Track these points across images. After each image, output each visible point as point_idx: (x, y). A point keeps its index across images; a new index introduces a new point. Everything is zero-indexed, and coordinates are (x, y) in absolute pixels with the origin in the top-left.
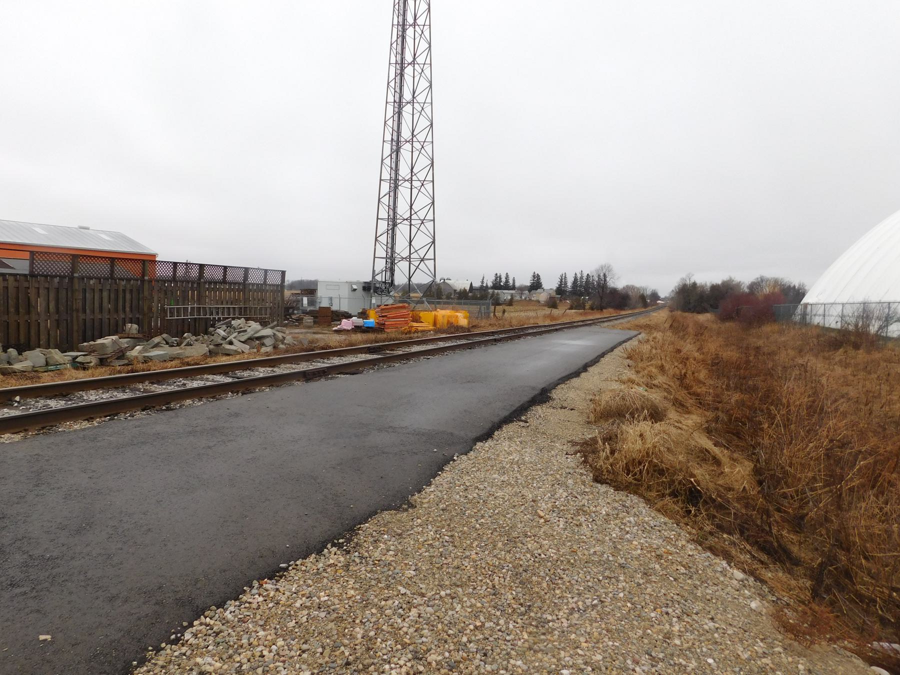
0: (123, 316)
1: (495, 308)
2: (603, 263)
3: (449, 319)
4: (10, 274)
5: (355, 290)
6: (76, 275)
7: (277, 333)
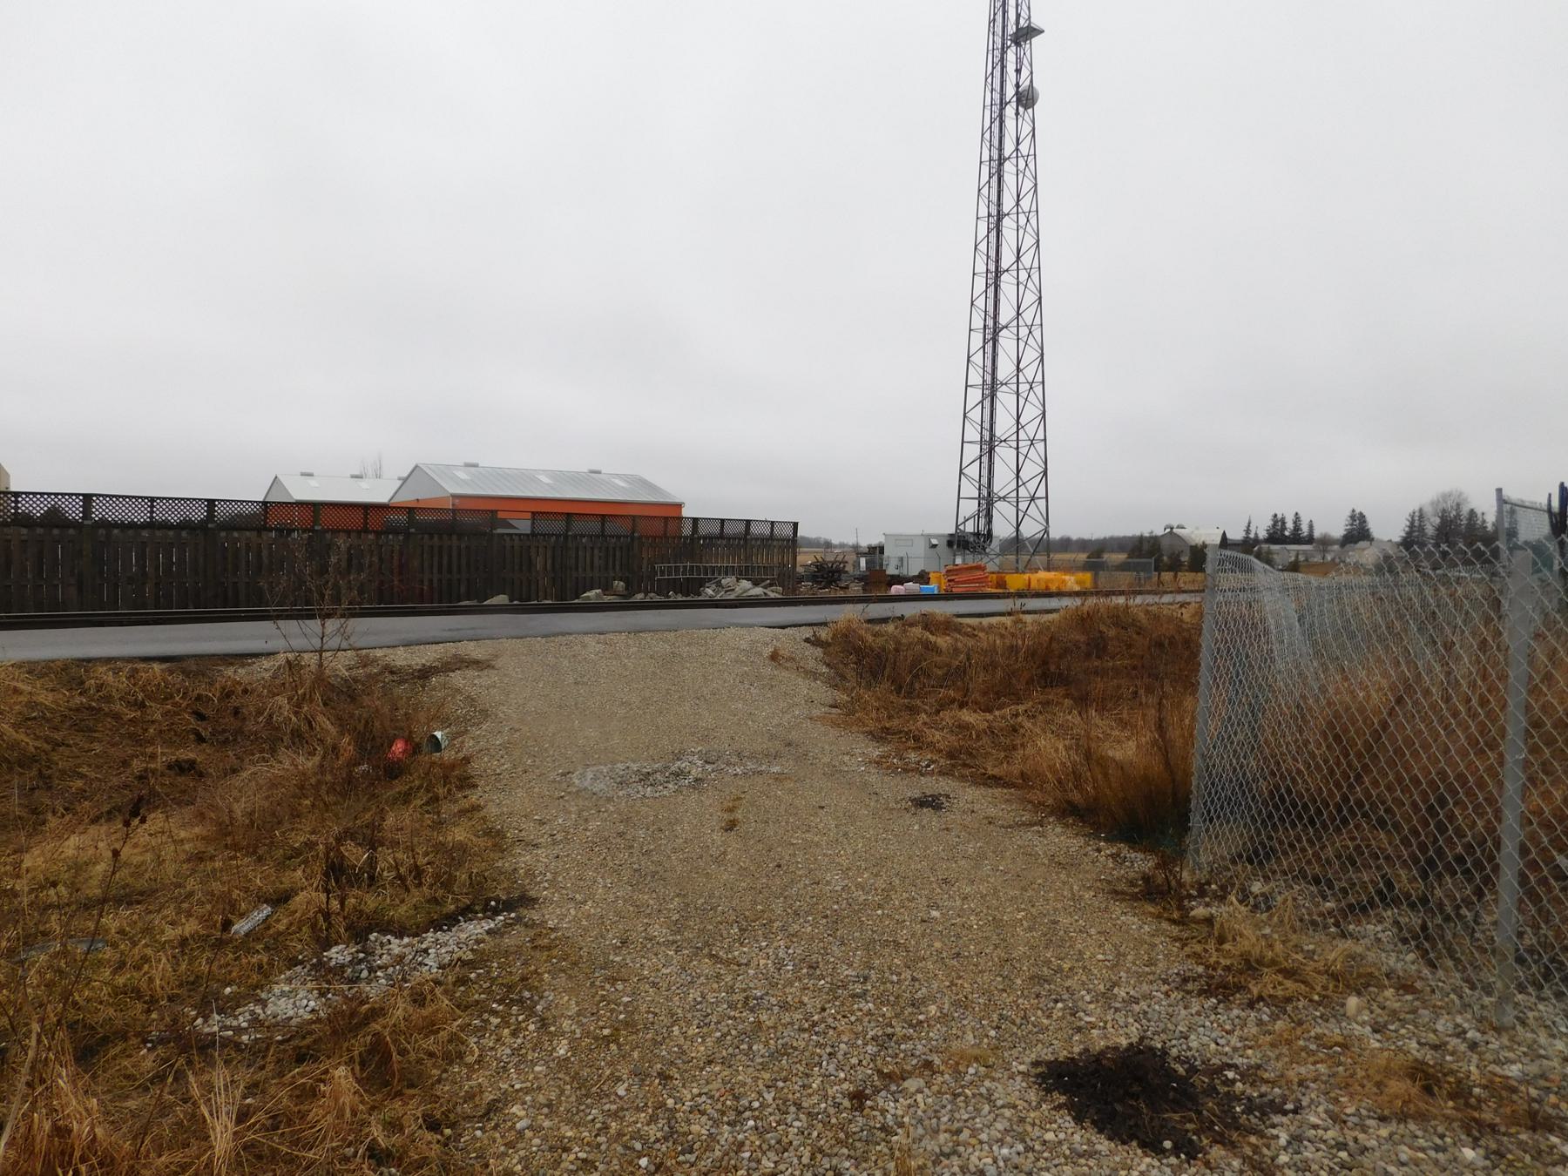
0: (612, 574)
1: (1159, 574)
2: (1447, 489)
3: (1050, 585)
4: (516, 534)
5: (935, 546)
6: (570, 533)
7: (769, 593)
